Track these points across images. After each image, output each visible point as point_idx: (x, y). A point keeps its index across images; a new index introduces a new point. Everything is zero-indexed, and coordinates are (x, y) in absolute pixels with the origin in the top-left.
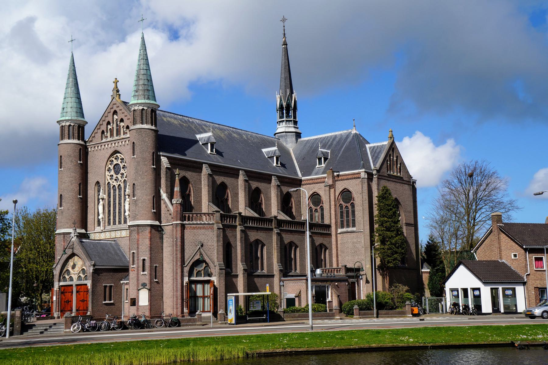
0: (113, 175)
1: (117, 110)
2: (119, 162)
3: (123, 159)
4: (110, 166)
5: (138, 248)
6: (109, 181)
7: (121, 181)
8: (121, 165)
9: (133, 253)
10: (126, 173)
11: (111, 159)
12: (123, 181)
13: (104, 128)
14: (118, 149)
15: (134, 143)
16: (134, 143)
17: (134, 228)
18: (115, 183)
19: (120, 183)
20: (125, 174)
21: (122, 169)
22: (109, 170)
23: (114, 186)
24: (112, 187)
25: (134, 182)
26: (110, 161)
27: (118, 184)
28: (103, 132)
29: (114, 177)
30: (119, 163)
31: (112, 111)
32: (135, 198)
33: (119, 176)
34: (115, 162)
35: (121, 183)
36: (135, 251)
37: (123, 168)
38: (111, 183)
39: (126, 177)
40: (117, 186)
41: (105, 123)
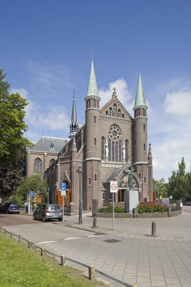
0: (112, 136)
1: (117, 104)
2: (116, 130)
3: (119, 129)
4: (110, 131)
5: (147, 175)
6: (110, 138)
7: (117, 140)
8: (118, 132)
9: (145, 177)
10: (120, 137)
11: (111, 127)
12: (119, 140)
13: (108, 109)
14: (117, 124)
15: (144, 125)
16: (144, 125)
17: (145, 165)
18: (114, 141)
19: (117, 141)
20: (120, 138)
21: (118, 134)
22: (110, 132)
23: (113, 141)
24: (112, 141)
25: (144, 143)
26: (110, 128)
27: (116, 141)
28: (107, 112)
29: (113, 137)
30: (116, 131)
31: (113, 103)
32: (145, 151)
33: (116, 137)
34: (113, 130)
35: (118, 141)
36: (146, 176)
37: (118, 134)
38: (111, 139)
39: (121, 139)
40: (115, 142)
41: (109, 108)
